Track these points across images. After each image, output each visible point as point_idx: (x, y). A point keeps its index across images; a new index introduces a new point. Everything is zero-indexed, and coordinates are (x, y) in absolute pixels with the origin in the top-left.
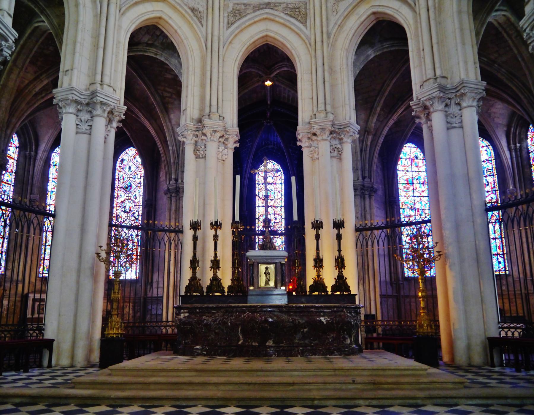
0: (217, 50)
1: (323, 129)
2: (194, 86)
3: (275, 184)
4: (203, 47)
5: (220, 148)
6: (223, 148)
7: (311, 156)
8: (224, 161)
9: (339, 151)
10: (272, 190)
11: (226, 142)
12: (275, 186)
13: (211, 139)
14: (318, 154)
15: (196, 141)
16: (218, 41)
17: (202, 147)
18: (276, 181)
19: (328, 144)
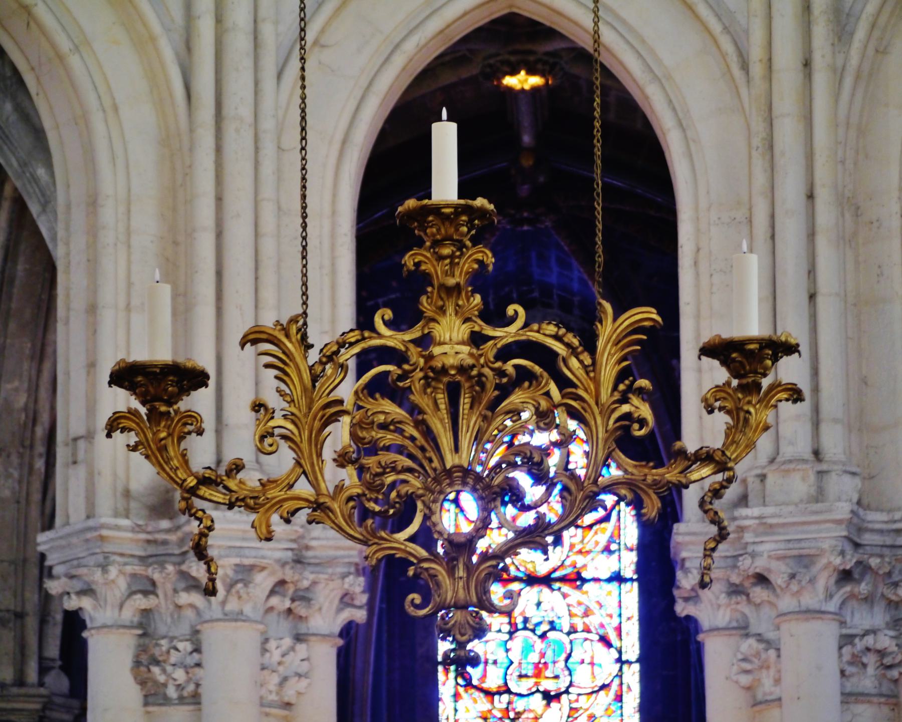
0: (246, 112)
1: (805, 560)
2: (128, 308)
3: (576, 579)
4: (168, 81)
5: (272, 645)
6: (288, 642)
7: (745, 680)
8: (288, 705)
9: (890, 667)
10: (553, 627)
11: (301, 609)
12: (575, 595)
13: (229, 607)
14: (777, 681)
15: (146, 613)
16: (248, 63)
17: (181, 646)
18: (580, 560)
19: (829, 632)
